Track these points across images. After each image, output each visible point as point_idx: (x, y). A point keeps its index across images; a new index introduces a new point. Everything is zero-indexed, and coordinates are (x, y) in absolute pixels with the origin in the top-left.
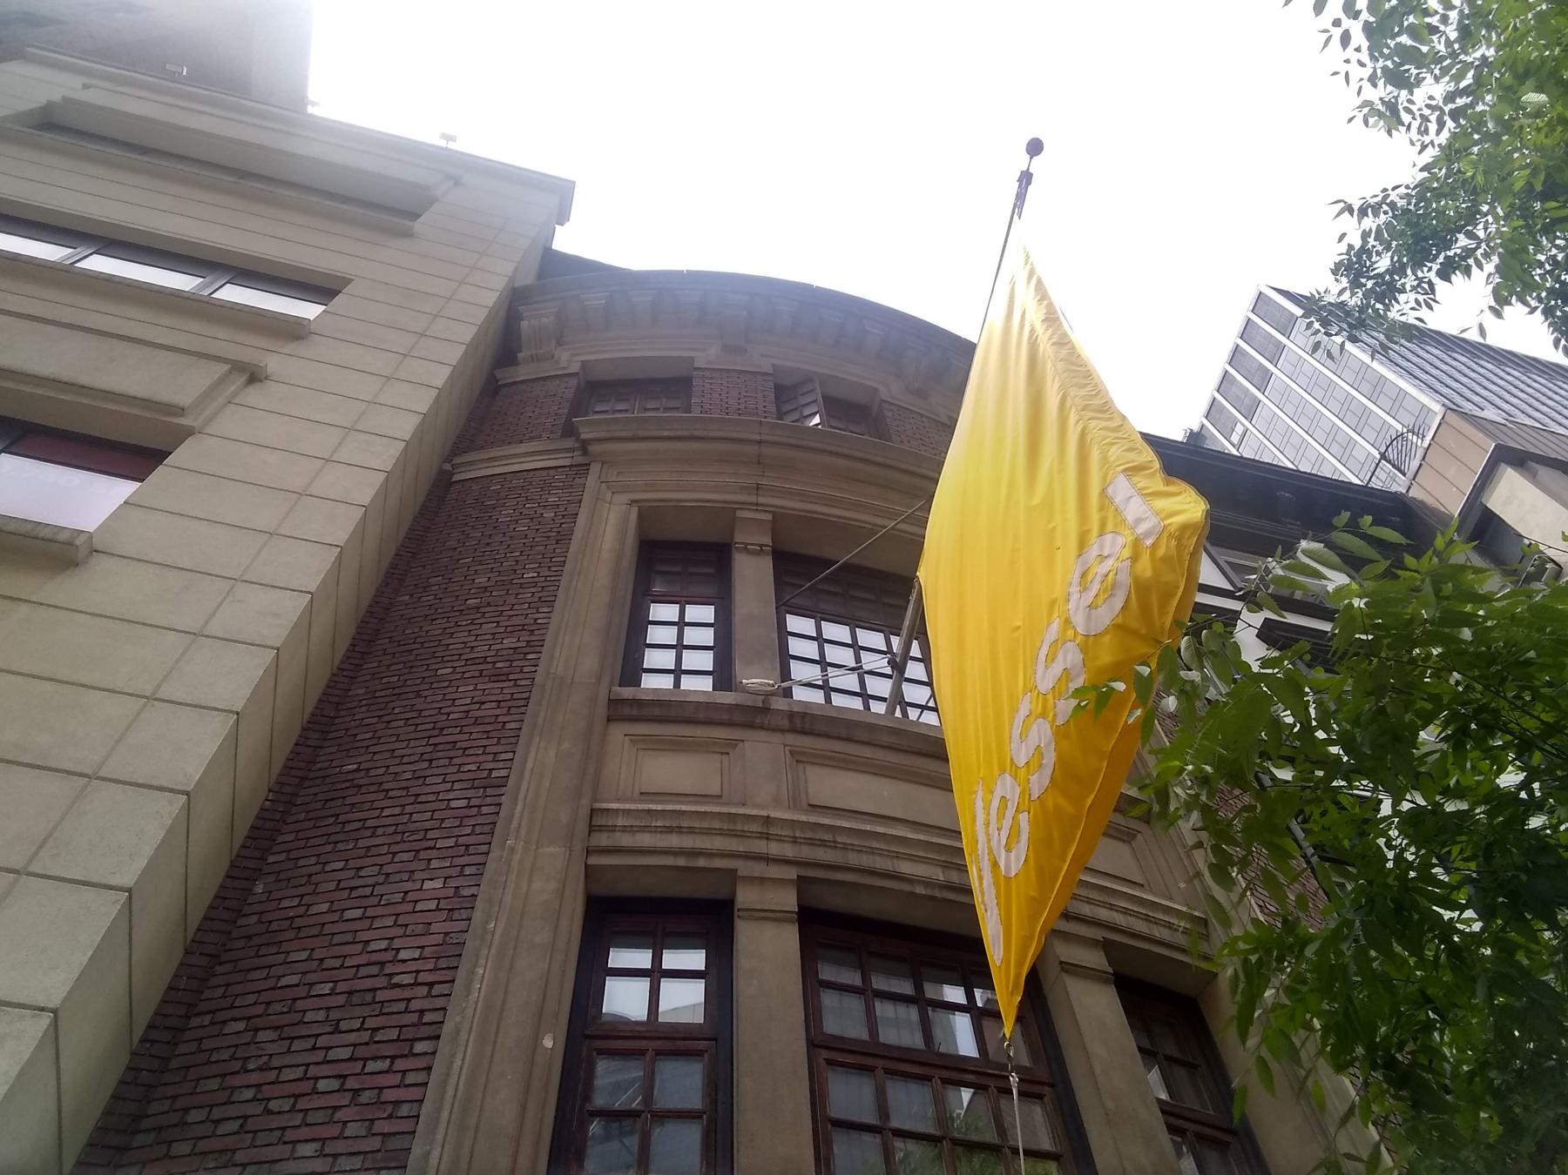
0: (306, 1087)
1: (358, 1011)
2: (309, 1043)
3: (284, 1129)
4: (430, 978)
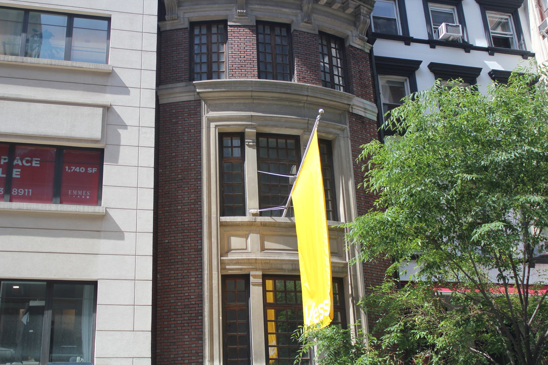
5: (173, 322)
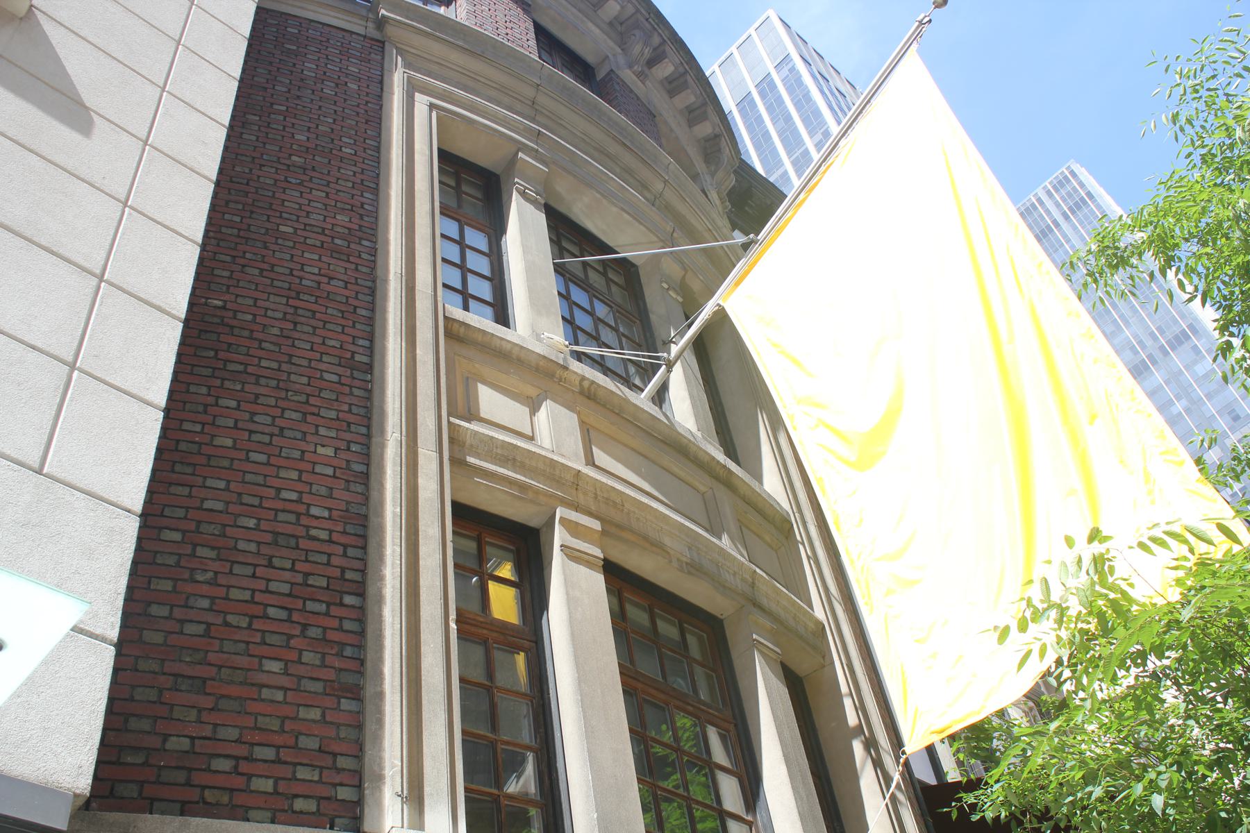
5: (205, 589)
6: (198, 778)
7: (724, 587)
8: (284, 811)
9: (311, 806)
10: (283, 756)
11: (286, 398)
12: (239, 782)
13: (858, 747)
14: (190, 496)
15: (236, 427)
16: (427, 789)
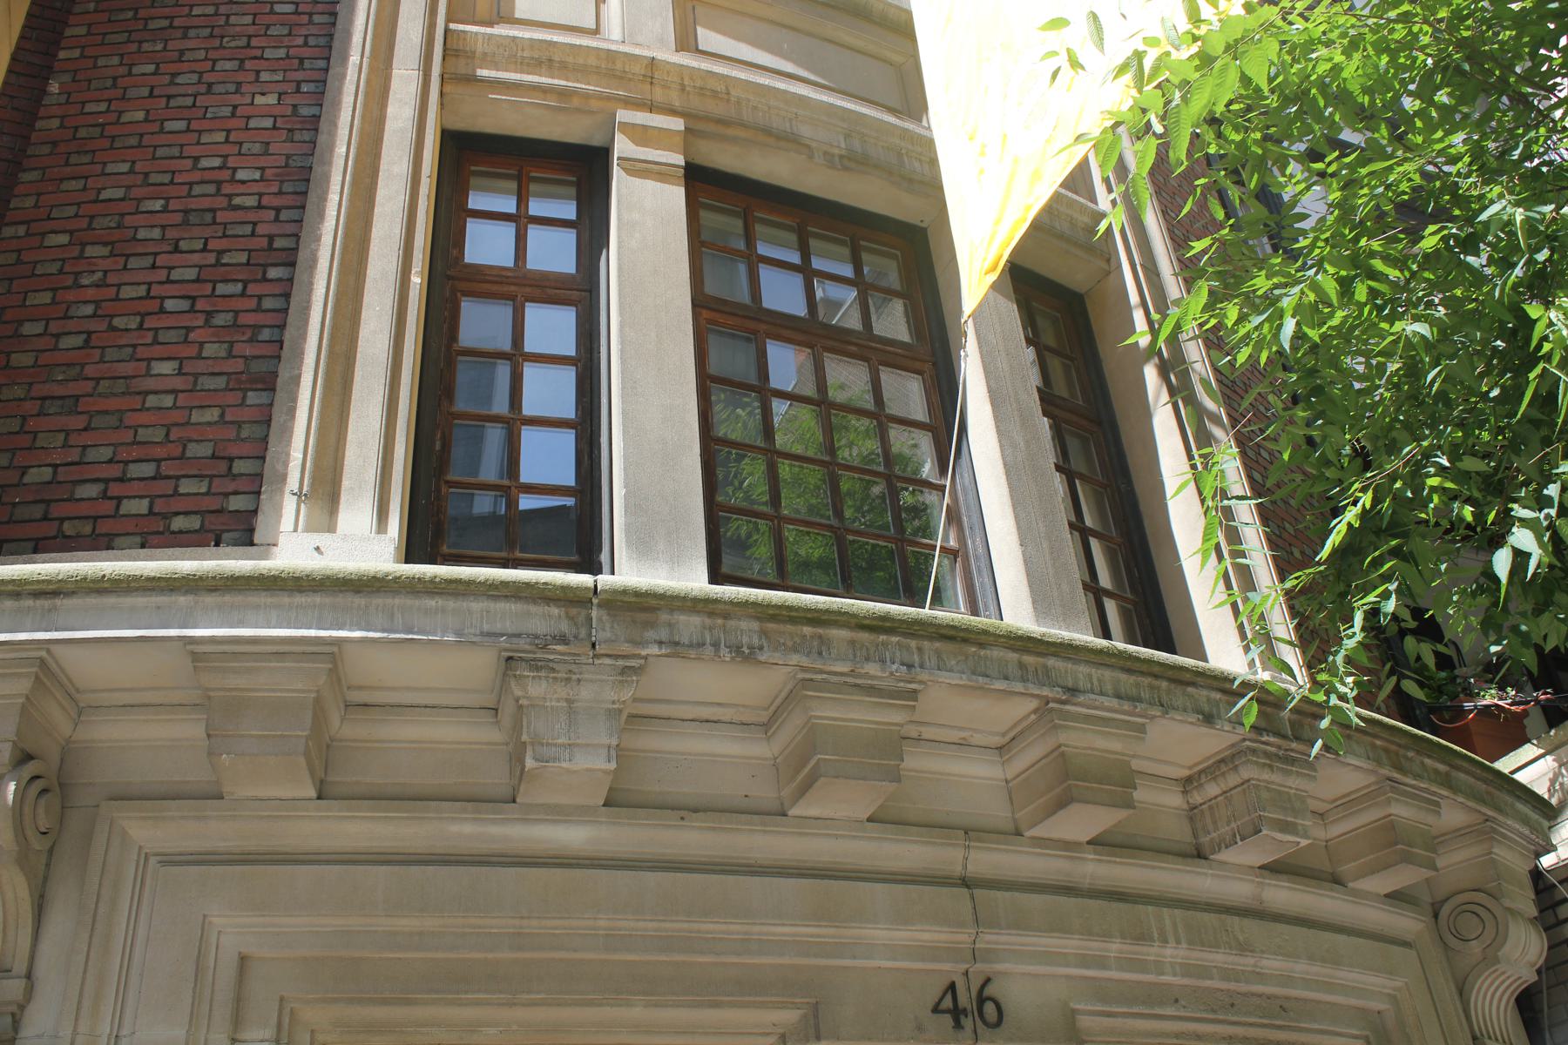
0: (153, 306)
1: (196, 232)
2: (148, 261)
3: (134, 346)
4: (277, 202)
6: (56, 511)
7: (911, 181)
8: (158, 533)
9: (194, 523)
10: (164, 470)
11: (221, 47)
12: (107, 507)
13: (1150, 373)
14: (85, 189)
15: (151, 95)
16: (346, 483)
